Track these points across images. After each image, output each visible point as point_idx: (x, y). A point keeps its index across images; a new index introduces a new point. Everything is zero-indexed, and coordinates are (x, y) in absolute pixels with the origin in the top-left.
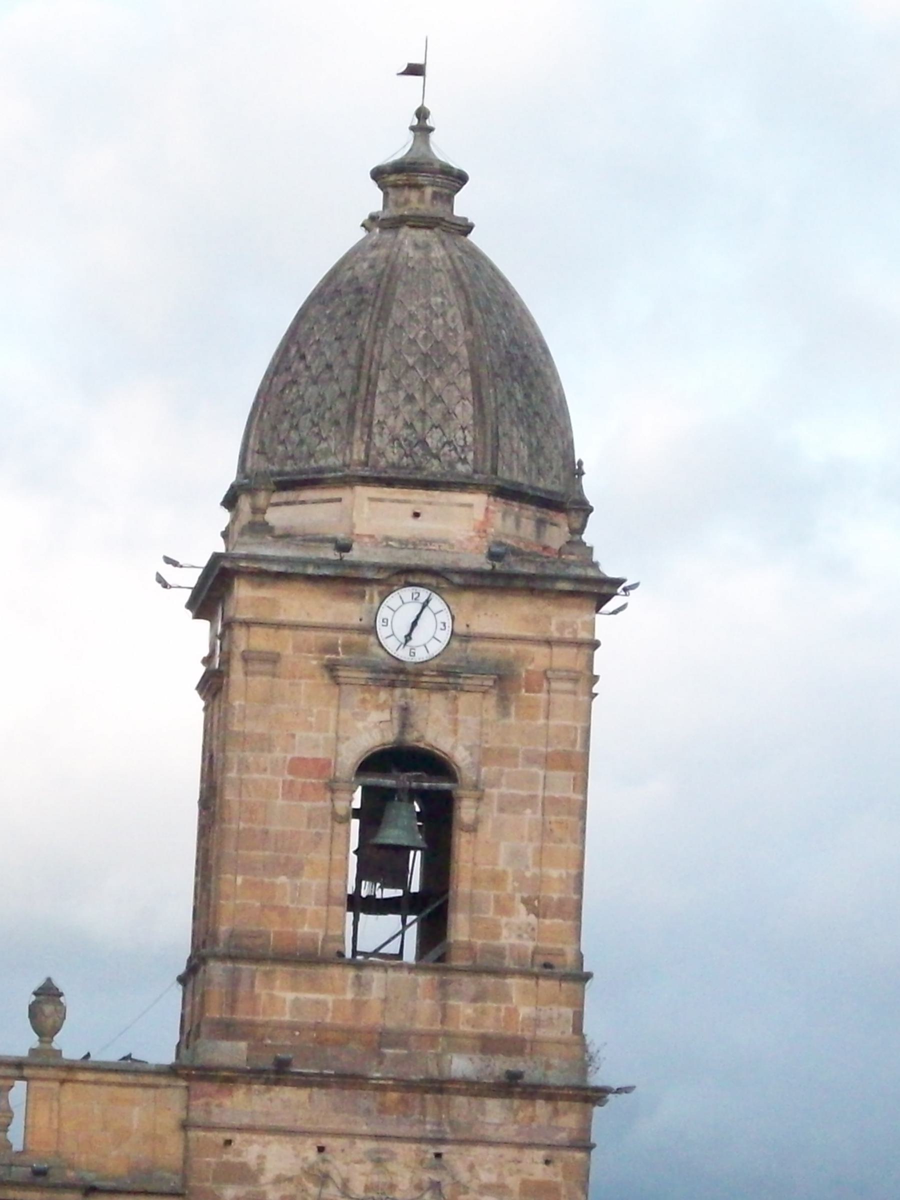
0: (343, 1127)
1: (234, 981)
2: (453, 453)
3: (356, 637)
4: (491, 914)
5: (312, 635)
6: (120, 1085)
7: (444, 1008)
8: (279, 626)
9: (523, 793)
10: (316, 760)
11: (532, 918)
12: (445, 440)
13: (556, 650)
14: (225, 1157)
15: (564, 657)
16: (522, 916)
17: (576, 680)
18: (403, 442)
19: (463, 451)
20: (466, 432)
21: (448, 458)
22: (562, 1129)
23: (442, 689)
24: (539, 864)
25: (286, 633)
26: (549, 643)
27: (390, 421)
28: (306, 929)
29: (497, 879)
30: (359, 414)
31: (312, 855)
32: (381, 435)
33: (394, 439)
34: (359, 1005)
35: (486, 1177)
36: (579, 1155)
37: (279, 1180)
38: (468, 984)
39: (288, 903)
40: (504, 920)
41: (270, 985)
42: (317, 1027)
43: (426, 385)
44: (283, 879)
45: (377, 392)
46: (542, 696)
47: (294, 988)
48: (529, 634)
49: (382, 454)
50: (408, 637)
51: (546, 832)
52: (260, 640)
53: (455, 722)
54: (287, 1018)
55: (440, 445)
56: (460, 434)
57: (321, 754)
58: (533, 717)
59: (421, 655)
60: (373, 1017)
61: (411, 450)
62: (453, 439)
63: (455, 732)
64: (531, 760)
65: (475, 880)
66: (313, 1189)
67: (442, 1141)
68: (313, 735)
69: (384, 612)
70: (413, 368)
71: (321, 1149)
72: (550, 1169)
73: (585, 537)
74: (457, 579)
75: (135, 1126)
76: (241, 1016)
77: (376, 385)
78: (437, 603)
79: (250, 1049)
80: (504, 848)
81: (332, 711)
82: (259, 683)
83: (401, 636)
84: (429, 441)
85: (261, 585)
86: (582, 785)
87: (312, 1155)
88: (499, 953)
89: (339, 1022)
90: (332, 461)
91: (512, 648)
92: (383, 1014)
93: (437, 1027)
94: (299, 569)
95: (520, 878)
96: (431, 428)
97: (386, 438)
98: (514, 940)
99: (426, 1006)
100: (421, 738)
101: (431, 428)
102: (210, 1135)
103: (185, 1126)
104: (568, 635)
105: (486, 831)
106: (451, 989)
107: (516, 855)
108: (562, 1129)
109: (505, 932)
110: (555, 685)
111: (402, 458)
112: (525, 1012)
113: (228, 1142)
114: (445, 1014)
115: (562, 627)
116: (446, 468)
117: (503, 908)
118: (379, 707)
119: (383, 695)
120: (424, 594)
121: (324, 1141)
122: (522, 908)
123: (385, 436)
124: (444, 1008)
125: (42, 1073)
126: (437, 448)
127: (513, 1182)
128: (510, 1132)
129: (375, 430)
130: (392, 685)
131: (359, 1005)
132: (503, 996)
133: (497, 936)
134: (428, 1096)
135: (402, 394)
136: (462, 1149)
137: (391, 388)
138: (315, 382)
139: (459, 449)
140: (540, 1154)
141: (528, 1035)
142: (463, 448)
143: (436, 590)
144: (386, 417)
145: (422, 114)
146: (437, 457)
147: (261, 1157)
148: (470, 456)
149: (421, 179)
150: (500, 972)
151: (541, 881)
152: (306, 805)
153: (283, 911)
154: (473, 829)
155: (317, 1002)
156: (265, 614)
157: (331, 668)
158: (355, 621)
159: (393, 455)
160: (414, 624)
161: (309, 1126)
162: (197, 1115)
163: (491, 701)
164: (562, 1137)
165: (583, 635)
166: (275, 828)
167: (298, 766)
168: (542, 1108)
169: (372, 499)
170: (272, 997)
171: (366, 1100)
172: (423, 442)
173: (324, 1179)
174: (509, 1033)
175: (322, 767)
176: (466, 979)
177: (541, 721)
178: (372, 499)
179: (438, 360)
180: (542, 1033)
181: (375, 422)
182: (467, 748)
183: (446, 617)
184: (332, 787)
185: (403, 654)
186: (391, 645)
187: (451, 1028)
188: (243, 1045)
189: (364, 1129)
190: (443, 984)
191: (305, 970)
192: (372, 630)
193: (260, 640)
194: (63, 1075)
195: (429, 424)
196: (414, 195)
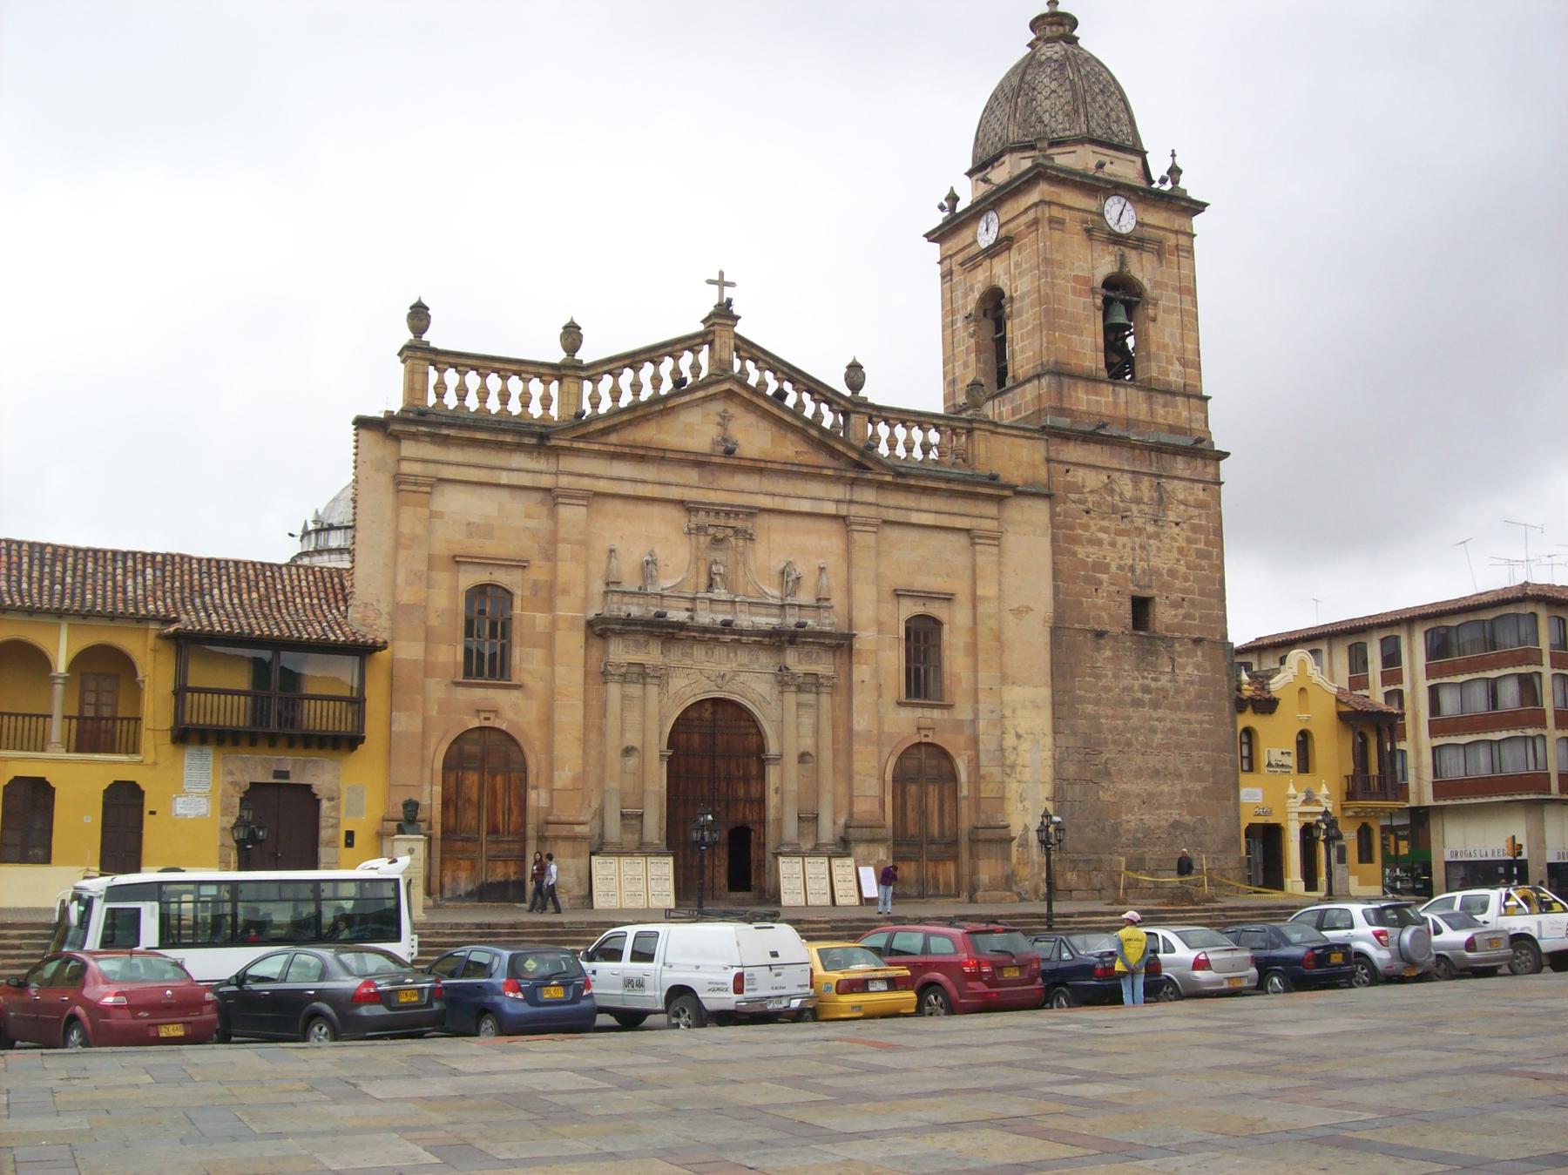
0: (1118, 467)
1: (1061, 386)
3: (1096, 218)
4: (1164, 364)
5: (1077, 214)
6: (1016, 436)
7: (1151, 409)
8: (1063, 206)
9: (1171, 305)
10: (1085, 277)
11: (1181, 368)
13: (1180, 237)
14: (1068, 479)
15: (1183, 240)
16: (1177, 367)
17: (1188, 252)
22: (1208, 474)
23: (1135, 248)
24: (1183, 341)
25: (1067, 211)
26: (1176, 232)
28: (1088, 364)
29: (1165, 347)
30: (1081, 110)
31: (1087, 325)
33: (1098, 125)
34: (1115, 404)
35: (1181, 497)
36: (1217, 487)
37: (1092, 492)
38: (1160, 399)
39: (1078, 349)
40: (1170, 368)
41: (1076, 391)
42: (1098, 414)
43: (1106, 103)
44: (1075, 336)
46: (1175, 258)
47: (1087, 394)
48: (1169, 227)
49: (1094, 131)
50: (1119, 220)
51: (1183, 326)
52: (1056, 212)
53: (1142, 265)
54: (1085, 408)
57: (1085, 274)
58: (1173, 268)
59: (1124, 231)
60: (1121, 412)
63: (1142, 270)
64: (1174, 290)
65: (1158, 346)
66: (1109, 499)
67: (1160, 476)
68: (1081, 263)
69: (1107, 207)
70: (1097, 94)
71: (1109, 477)
72: (1205, 493)
73: (1180, 185)
74: (1141, 194)
75: (1025, 459)
76: (1066, 405)
78: (1128, 206)
79: (1073, 422)
80: (1167, 331)
81: (1089, 253)
82: (1057, 235)
83: (1116, 219)
85: (1052, 185)
86: (1195, 304)
87: (1106, 480)
88: (1169, 383)
89: (1108, 413)
90: (1067, 133)
91: (1161, 233)
92: (1127, 409)
93: (1150, 418)
94: (1073, 178)
95: (1174, 347)
98: (1175, 378)
99: (1144, 407)
100: (1129, 272)
102: (1060, 466)
103: (1048, 460)
104: (1182, 228)
105: (1159, 319)
106: (1154, 399)
107: (1172, 335)
108: (1208, 474)
109: (1171, 374)
110: (1181, 253)
112: (1185, 414)
113: (1068, 471)
114: (1152, 412)
115: (1180, 225)
117: (1169, 362)
118: (1110, 254)
119: (1110, 248)
120: (1123, 201)
121: (1110, 473)
122: (1177, 363)
124: (1151, 409)
125: (983, 426)
127: (1191, 499)
128: (1187, 474)
130: (1115, 243)
131: (1115, 404)
132: (1175, 406)
133: (1168, 376)
134: (1152, 453)
136: (1170, 481)
138: (1046, 98)
140: (1201, 486)
141: (1187, 426)
143: (1128, 199)
146: (1117, 136)
147: (1083, 479)
149: (1066, 21)
150: (1174, 394)
151: (1184, 350)
152: (1082, 299)
153: (1077, 353)
154: (1154, 320)
155: (1098, 402)
156: (1055, 198)
157: (1088, 231)
158: (1094, 209)
159: (1099, 132)
160: (1121, 214)
161: (1102, 465)
162: (1053, 455)
163: (1155, 259)
164: (1209, 478)
165: (1189, 230)
166: (1068, 310)
167: (1076, 278)
168: (1199, 462)
169: (1094, 152)
170: (1077, 397)
171: (1126, 453)
172: (1110, 128)
173: (1112, 492)
174: (1179, 424)
175: (1087, 281)
176: (1159, 395)
177: (1176, 270)
178: (1094, 152)
180: (1194, 425)
182: (1149, 280)
183: (1132, 213)
184: (1093, 291)
185: (1116, 229)
186: (1111, 223)
187: (1155, 420)
188: (1068, 420)
189: (1126, 468)
190: (1150, 397)
191: (1090, 384)
192: (1102, 215)
193: (1056, 212)
194: (992, 428)
196: (1061, 29)
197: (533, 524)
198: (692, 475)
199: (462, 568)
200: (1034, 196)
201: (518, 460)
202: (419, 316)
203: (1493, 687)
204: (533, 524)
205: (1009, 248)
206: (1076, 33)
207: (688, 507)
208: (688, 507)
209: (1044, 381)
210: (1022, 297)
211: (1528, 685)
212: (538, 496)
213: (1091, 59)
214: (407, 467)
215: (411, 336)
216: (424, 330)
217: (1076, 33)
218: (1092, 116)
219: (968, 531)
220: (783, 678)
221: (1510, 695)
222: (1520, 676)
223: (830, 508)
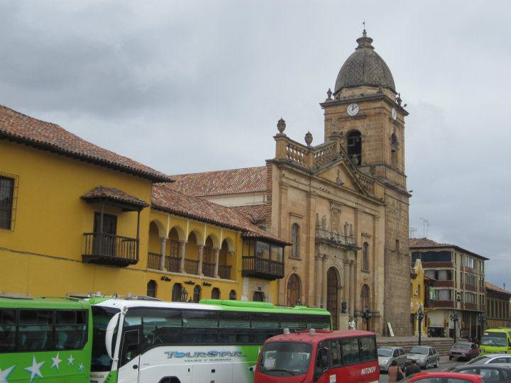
145: (365, 31)
197: (303, 203)
198: (332, 190)
199: (292, 217)
200: (378, 104)
201: (303, 181)
202: (281, 125)
203: (436, 274)
204: (303, 203)
205: (365, 119)
206: (372, 44)
207: (331, 201)
208: (331, 201)
209: (381, 167)
210: (370, 136)
211: (449, 274)
212: (304, 194)
213: (378, 58)
214: (284, 180)
215: (279, 132)
216: (284, 129)
217: (372, 44)
219: (373, 215)
220: (345, 262)
221: (443, 276)
222: (447, 271)
223: (354, 205)
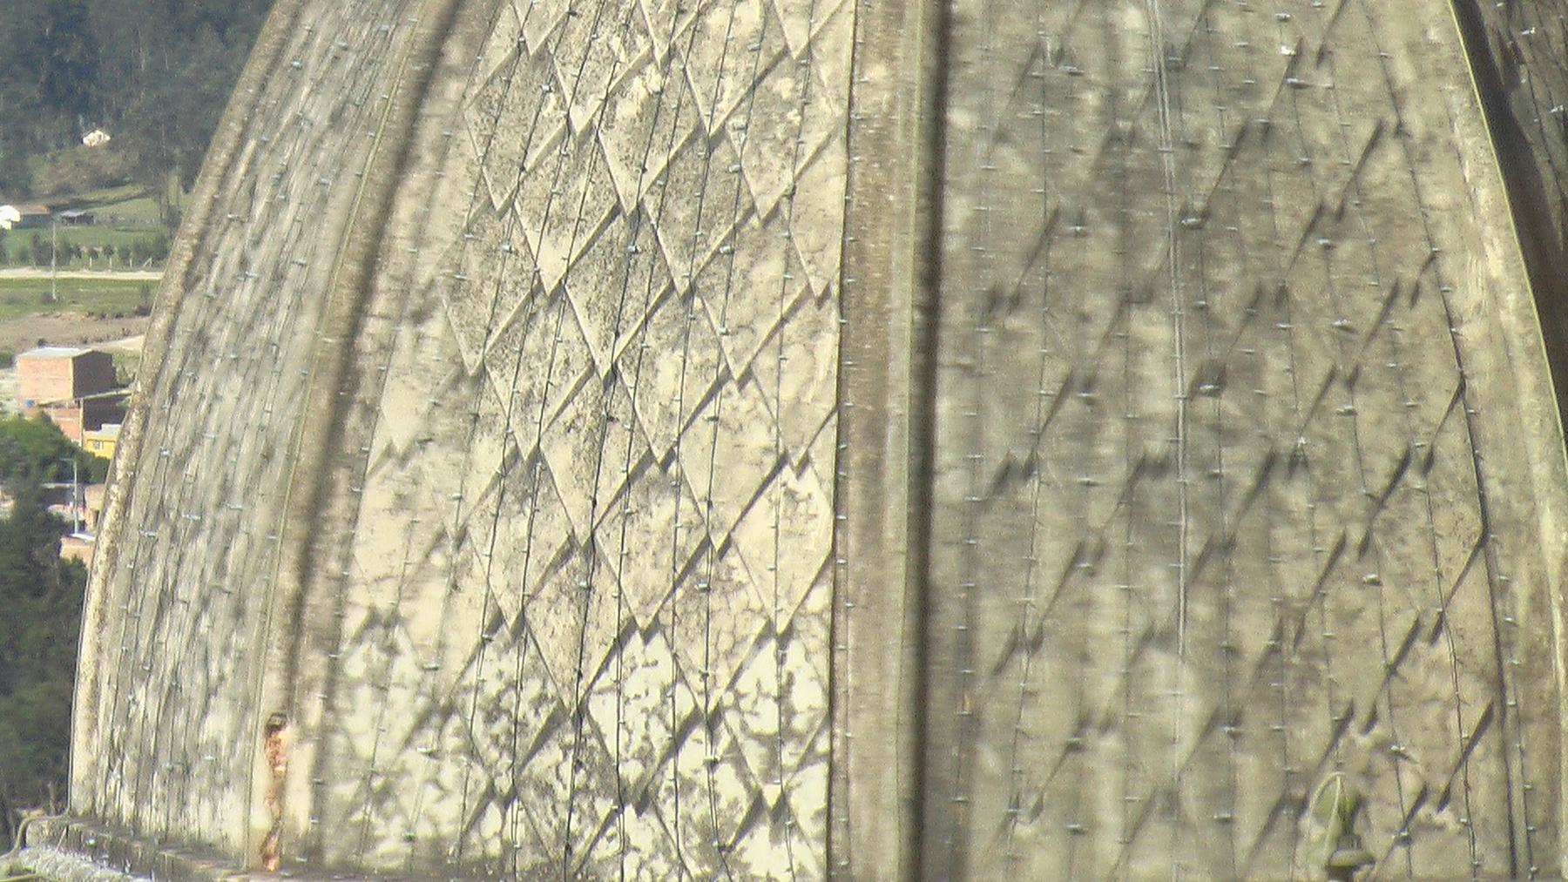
2: (726, 772)
12: (685, 703)
18: (478, 728)
19: (773, 766)
20: (795, 649)
21: (700, 809)
27: (425, 614)
32: (380, 685)
45: (378, 447)
55: (660, 737)
56: (763, 667)
61: (516, 769)
62: (729, 699)
77: (371, 412)
84: (603, 711)
96: (620, 643)
97: (404, 707)
101: (620, 643)
111: (481, 812)
116: (691, 864)
123: (397, 695)
126: (644, 757)
129: (356, 665)
135: (488, 455)
137: (443, 425)
139: (754, 756)
142: (773, 744)
144: (409, 587)
148: (809, 794)
179: (690, 247)
181: (354, 621)
195: (608, 619)
218: (383, 623)
